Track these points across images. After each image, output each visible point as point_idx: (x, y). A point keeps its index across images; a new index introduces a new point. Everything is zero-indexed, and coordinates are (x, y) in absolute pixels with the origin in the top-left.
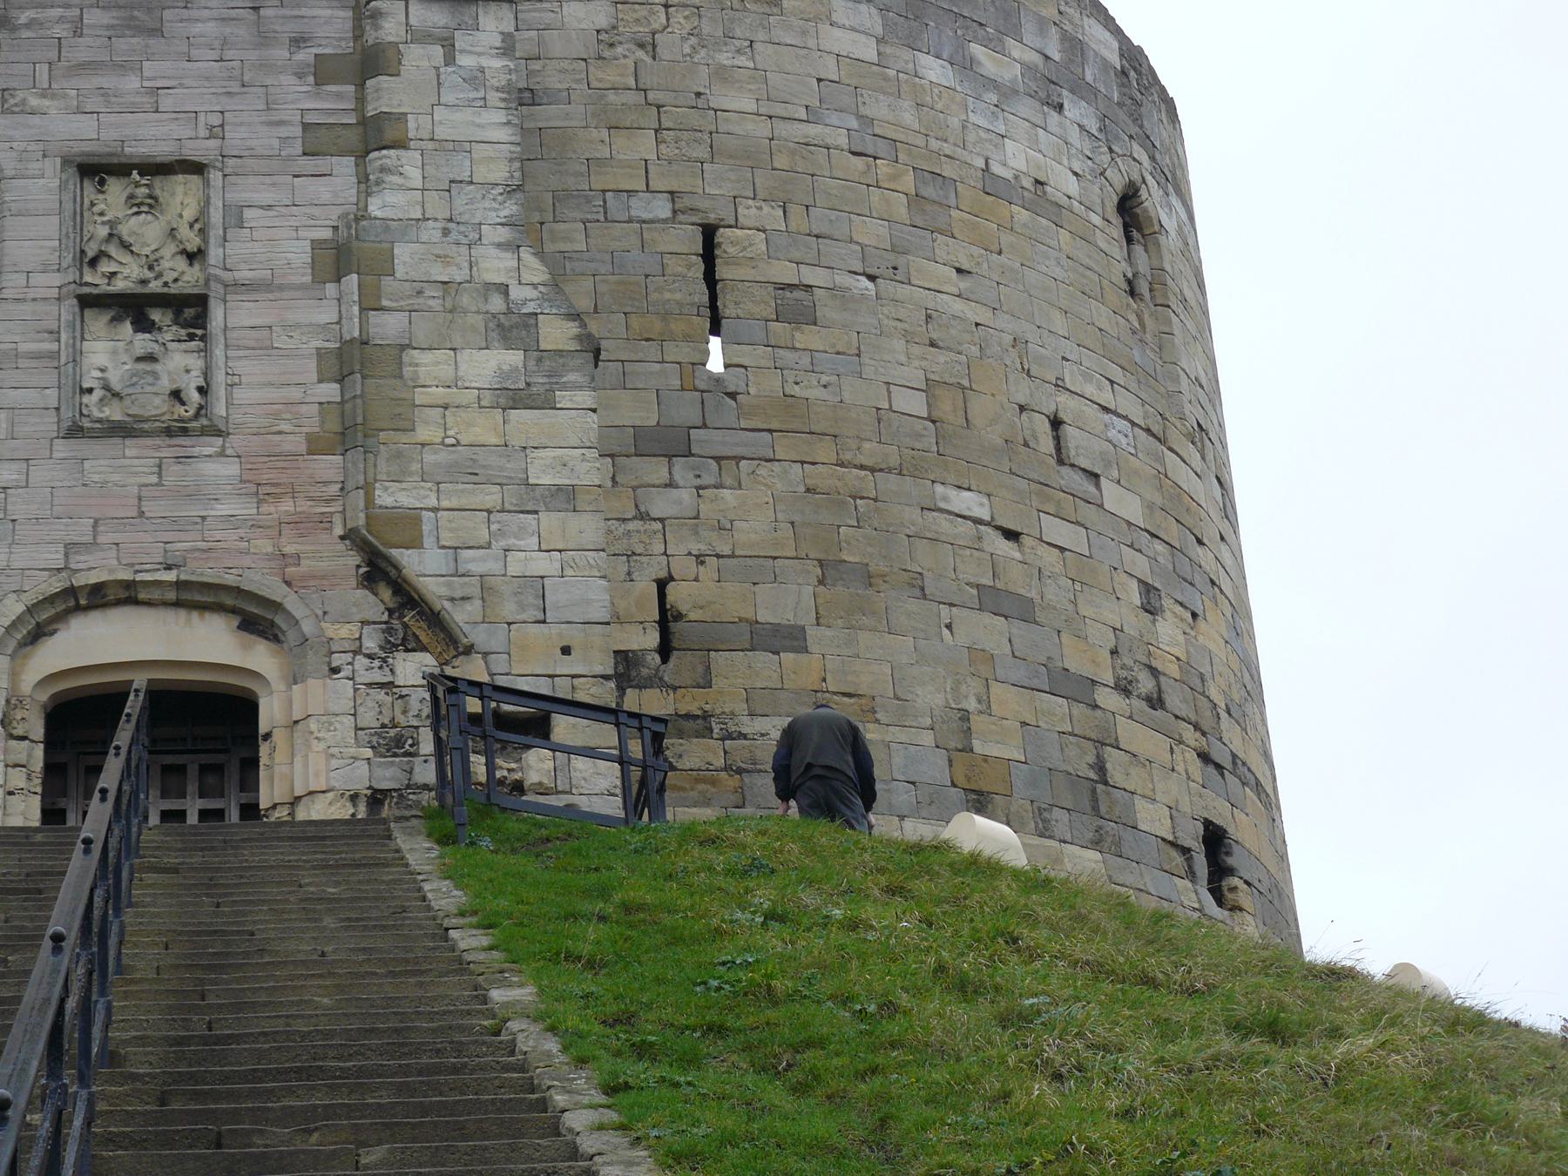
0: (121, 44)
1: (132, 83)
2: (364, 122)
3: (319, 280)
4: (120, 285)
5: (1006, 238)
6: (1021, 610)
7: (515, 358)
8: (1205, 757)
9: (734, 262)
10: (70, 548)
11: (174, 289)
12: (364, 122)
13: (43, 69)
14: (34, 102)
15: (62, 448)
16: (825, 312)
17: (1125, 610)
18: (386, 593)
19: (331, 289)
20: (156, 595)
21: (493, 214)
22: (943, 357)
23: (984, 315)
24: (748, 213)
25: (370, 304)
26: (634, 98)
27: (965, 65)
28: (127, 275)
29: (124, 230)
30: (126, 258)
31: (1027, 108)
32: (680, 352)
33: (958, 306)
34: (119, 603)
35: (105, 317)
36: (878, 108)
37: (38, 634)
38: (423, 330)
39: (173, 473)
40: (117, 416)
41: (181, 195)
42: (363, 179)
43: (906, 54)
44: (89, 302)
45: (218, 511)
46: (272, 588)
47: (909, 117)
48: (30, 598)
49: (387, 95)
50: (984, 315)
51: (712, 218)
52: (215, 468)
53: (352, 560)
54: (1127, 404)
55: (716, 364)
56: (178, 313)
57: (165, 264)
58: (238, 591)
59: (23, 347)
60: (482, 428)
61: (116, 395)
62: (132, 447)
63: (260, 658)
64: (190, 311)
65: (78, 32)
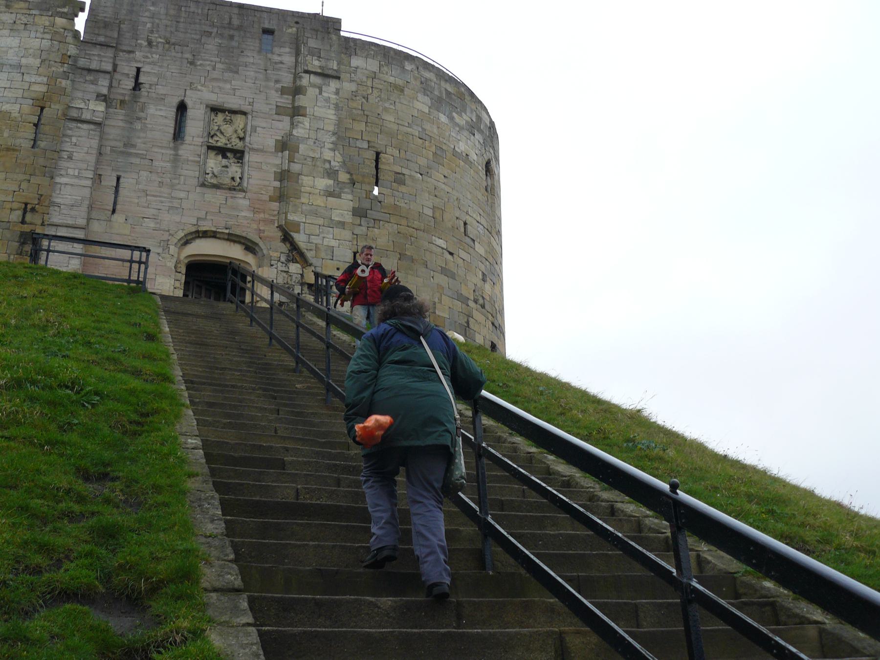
0: (226, 74)
1: (228, 86)
2: (294, 107)
3: (276, 151)
4: (219, 144)
5: (458, 169)
6: (450, 274)
7: (331, 182)
8: (493, 324)
9: (384, 163)
10: (198, 219)
11: (235, 148)
12: (294, 107)
13: (203, 79)
14: (199, 87)
15: (199, 189)
16: (408, 181)
17: (477, 280)
18: (288, 245)
19: (280, 154)
20: (222, 236)
21: (329, 139)
22: (438, 200)
23: (450, 190)
24: (389, 150)
26: (360, 112)
27: (451, 119)
28: (221, 142)
29: (222, 128)
30: (222, 137)
31: (466, 133)
32: (366, 187)
33: (443, 186)
34: (211, 237)
35: (214, 153)
36: (427, 126)
37: (187, 243)
38: (305, 171)
39: (230, 201)
40: (215, 182)
41: (239, 120)
42: (292, 124)
43: (436, 112)
44: (210, 148)
45: (242, 214)
46: (256, 239)
47: (435, 131)
48: (186, 232)
49: (302, 100)
50: (450, 190)
51: (379, 150)
52: (242, 202)
53: (280, 234)
54: (483, 221)
55: (376, 191)
56: (235, 155)
57: (233, 140)
58: (246, 238)
59: (191, 158)
60: (320, 201)
61: (216, 176)
62: (219, 192)
63: (250, 259)
64: (239, 155)
65: (214, 69)
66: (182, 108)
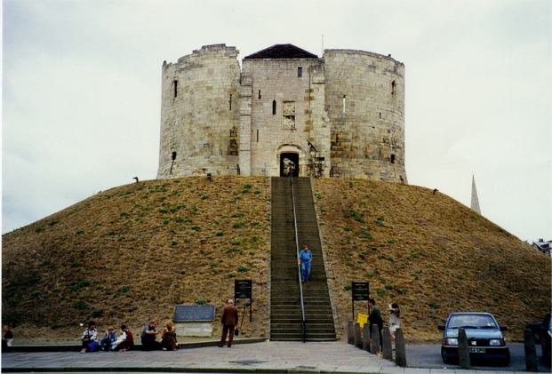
25: (310, 117)
41: (293, 104)
46: (299, 144)
49: (312, 94)
52: (295, 133)
66: (274, 103)
